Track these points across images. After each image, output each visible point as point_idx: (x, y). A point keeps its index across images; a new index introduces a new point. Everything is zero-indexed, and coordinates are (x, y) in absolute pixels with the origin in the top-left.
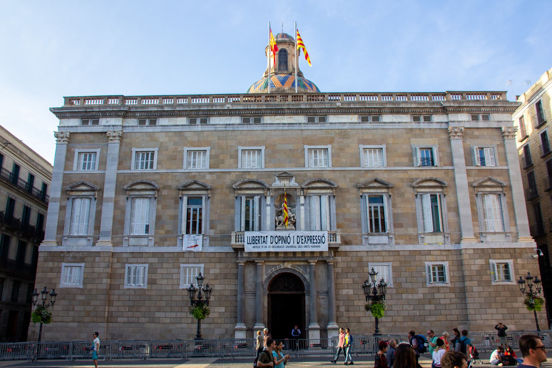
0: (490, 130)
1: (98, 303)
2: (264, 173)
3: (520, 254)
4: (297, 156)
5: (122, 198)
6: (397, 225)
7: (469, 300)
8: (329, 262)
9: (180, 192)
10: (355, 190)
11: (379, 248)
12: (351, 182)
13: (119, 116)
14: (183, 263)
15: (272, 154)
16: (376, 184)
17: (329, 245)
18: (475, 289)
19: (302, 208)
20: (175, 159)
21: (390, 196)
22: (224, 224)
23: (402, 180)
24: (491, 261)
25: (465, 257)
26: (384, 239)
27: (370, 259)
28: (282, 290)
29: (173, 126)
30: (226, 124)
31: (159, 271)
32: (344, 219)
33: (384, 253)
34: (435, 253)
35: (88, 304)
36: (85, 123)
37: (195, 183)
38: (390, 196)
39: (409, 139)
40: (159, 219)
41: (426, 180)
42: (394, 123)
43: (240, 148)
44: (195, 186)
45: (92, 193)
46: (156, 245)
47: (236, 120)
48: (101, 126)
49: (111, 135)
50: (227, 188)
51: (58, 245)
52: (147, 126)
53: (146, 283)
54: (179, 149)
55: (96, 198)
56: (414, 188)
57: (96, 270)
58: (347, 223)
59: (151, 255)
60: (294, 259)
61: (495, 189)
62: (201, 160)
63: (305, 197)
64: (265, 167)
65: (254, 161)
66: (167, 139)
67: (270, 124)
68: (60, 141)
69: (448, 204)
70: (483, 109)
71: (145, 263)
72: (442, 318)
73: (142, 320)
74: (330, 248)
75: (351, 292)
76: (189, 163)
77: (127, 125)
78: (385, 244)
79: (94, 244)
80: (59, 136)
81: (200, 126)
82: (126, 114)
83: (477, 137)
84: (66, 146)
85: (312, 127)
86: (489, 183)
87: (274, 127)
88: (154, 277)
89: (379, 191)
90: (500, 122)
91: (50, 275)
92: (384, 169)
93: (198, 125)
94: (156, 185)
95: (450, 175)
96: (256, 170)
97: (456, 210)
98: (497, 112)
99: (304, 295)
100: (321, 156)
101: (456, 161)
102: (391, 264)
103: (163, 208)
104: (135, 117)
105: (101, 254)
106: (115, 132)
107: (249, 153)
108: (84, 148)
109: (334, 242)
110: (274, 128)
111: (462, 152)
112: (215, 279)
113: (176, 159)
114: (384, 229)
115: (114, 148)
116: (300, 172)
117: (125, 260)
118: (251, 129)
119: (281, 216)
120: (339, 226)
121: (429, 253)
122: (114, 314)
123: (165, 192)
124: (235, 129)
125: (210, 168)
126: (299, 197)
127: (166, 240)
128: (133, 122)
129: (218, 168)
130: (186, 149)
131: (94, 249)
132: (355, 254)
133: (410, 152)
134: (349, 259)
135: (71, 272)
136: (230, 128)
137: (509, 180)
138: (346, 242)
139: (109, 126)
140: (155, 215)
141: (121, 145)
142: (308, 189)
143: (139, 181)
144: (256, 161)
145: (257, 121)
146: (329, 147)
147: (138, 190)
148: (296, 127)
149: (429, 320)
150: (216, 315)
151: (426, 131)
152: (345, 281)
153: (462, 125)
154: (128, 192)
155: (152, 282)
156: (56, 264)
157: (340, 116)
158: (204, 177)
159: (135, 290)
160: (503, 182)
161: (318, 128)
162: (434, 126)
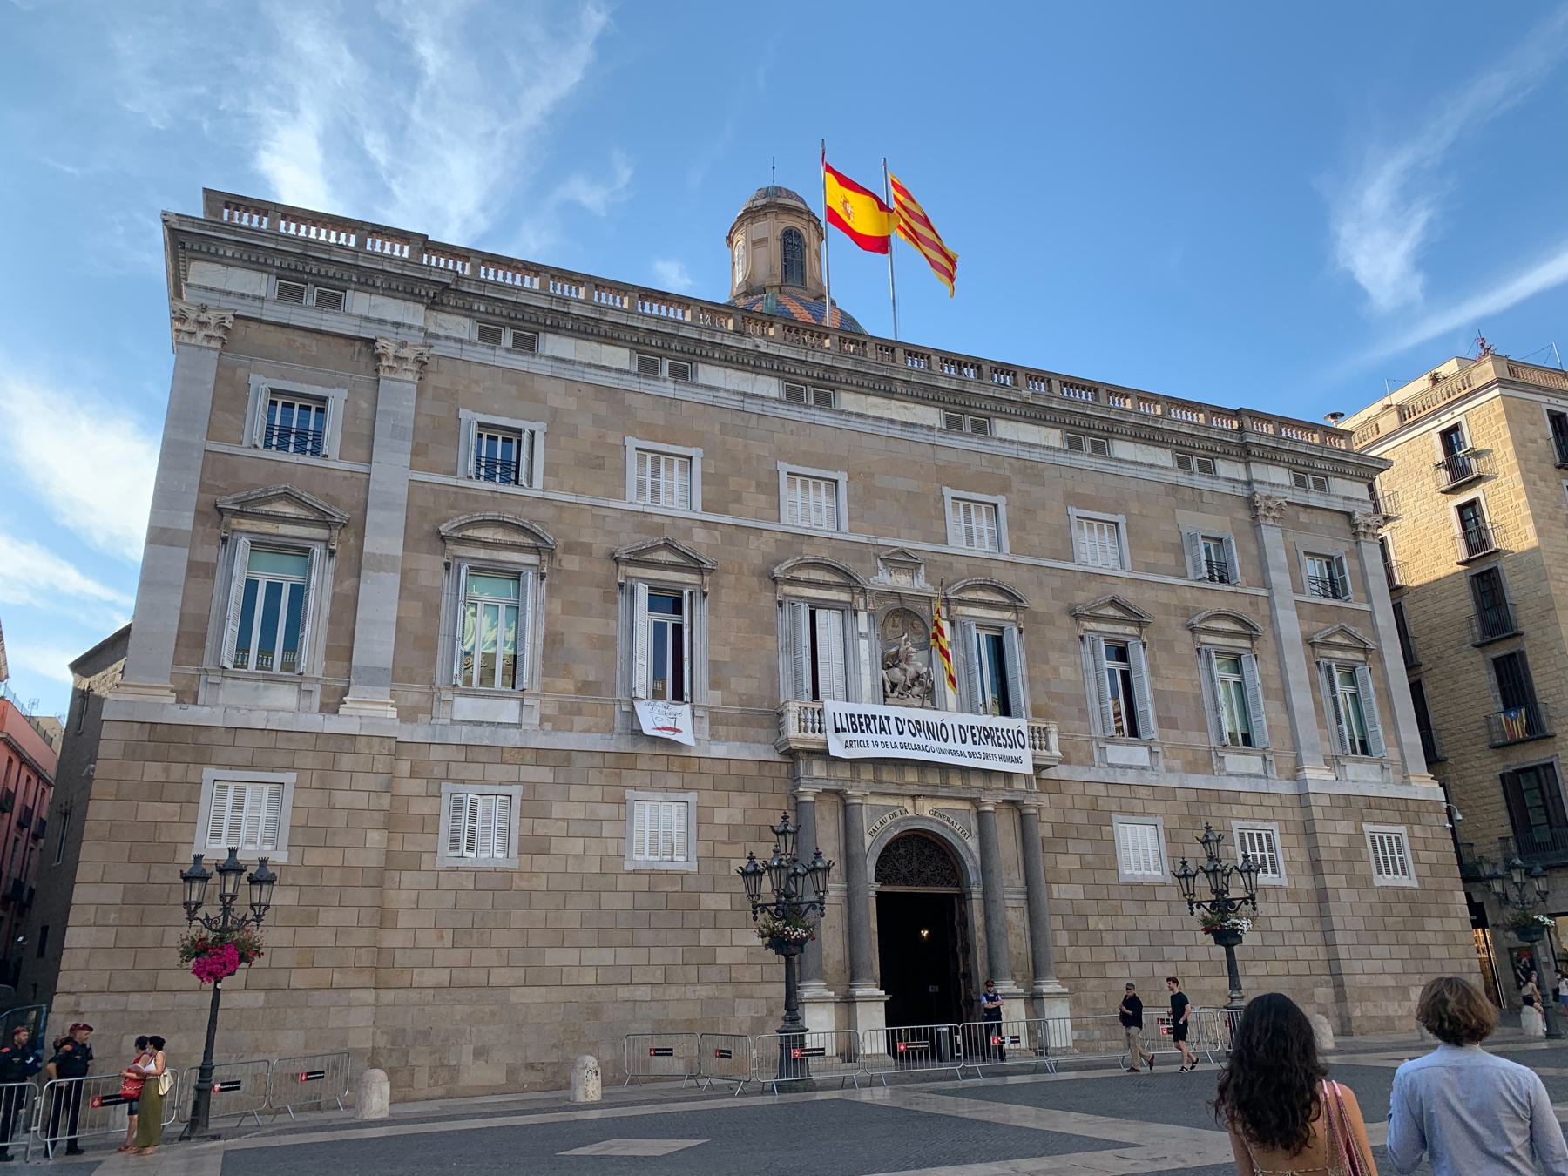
1: (349, 917)
2: (848, 546)
5: (429, 564)
6: (1165, 722)
7: (1337, 924)
8: (1029, 806)
9: (622, 568)
10: (1067, 621)
11: (1130, 778)
14: (635, 788)
15: (865, 499)
16: (1111, 612)
18: (1344, 894)
20: (601, 467)
23: (1165, 607)
24: (1368, 828)
25: (1317, 813)
26: (1139, 755)
28: (906, 882)
29: (590, 365)
30: (745, 394)
31: (558, 810)
33: (1143, 791)
34: (1249, 799)
35: (310, 921)
36: (290, 294)
37: (668, 546)
40: (554, 642)
41: (1219, 616)
42: (1141, 464)
43: (784, 467)
44: (663, 556)
45: (321, 533)
46: (548, 726)
47: (770, 387)
48: (351, 315)
49: (391, 351)
51: (179, 701)
52: (508, 350)
53: (514, 852)
54: (611, 441)
55: (332, 553)
56: (1192, 629)
57: (341, 799)
59: (529, 757)
60: (943, 792)
61: (1350, 656)
62: (676, 482)
63: (952, 624)
65: (818, 510)
66: (571, 403)
67: (857, 414)
68: (192, 334)
70: (1318, 464)
71: (510, 783)
72: (1279, 967)
73: (500, 976)
75: (1076, 892)
76: (641, 486)
77: (441, 332)
78: (1143, 768)
79: (331, 707)
80: (192, 316)
81: (670, 385)
82: (440, 296)
83: (1305, 528)
84: (216, 354)
85: (956, 441)
86: (1338, 639)
87: (867, 426)
88: (540, 831)
89: (1119, 629)
90: (1349, 499)
91: (150, 811)
92: (1126, 575)
93: (665, 380)
94: (550, 538)
95: (1263, 608)
98: (1342, 475)
99: (963, 897)
100: (981, 523)
102: (1160, 820)
103: (563, 613)
104: (467, 312)
105: (361, 745)
106: (403, 345)
107: (805, 486)
108: (283, 378)
110: (868, 429)
112: (731, 842)
114: (1134, 732)
115: (400, 397)
116: (936, 557)
117: (439, 771)
118: (809, 419)
121: (1235, 798)
122: (398, 953)
123: (571, 563)
124: (769, 410)
127: (580, 714)
128: (461, 326)
129: (726, 512)
130: (632, 443)
131: (332, 725)
132: (1078, 789)
133: (1176, 539)
135: (238, 804)
136: (754, 406)
137: (1377, 638)
139: (381, 321)
140: (541, 631)
141: (420, 392)
142: (962, 602)
143: (492, 514)
144: (824, 510)
145: (824, 401)
146: (1000, 500)
147: (485, 544)
148: (920, 436)
149: (1254, 971)
150: (740, 956)
151: (1207, 497)
152: (1065, 862)
153: (1276, 493)
154: (450, 547)
155: (534, 846)
156: (177, 771)
158: (688, 533)
159: (476, 873)
160: (1367, 640)
161: (973, 447)
162: (1226, 488)
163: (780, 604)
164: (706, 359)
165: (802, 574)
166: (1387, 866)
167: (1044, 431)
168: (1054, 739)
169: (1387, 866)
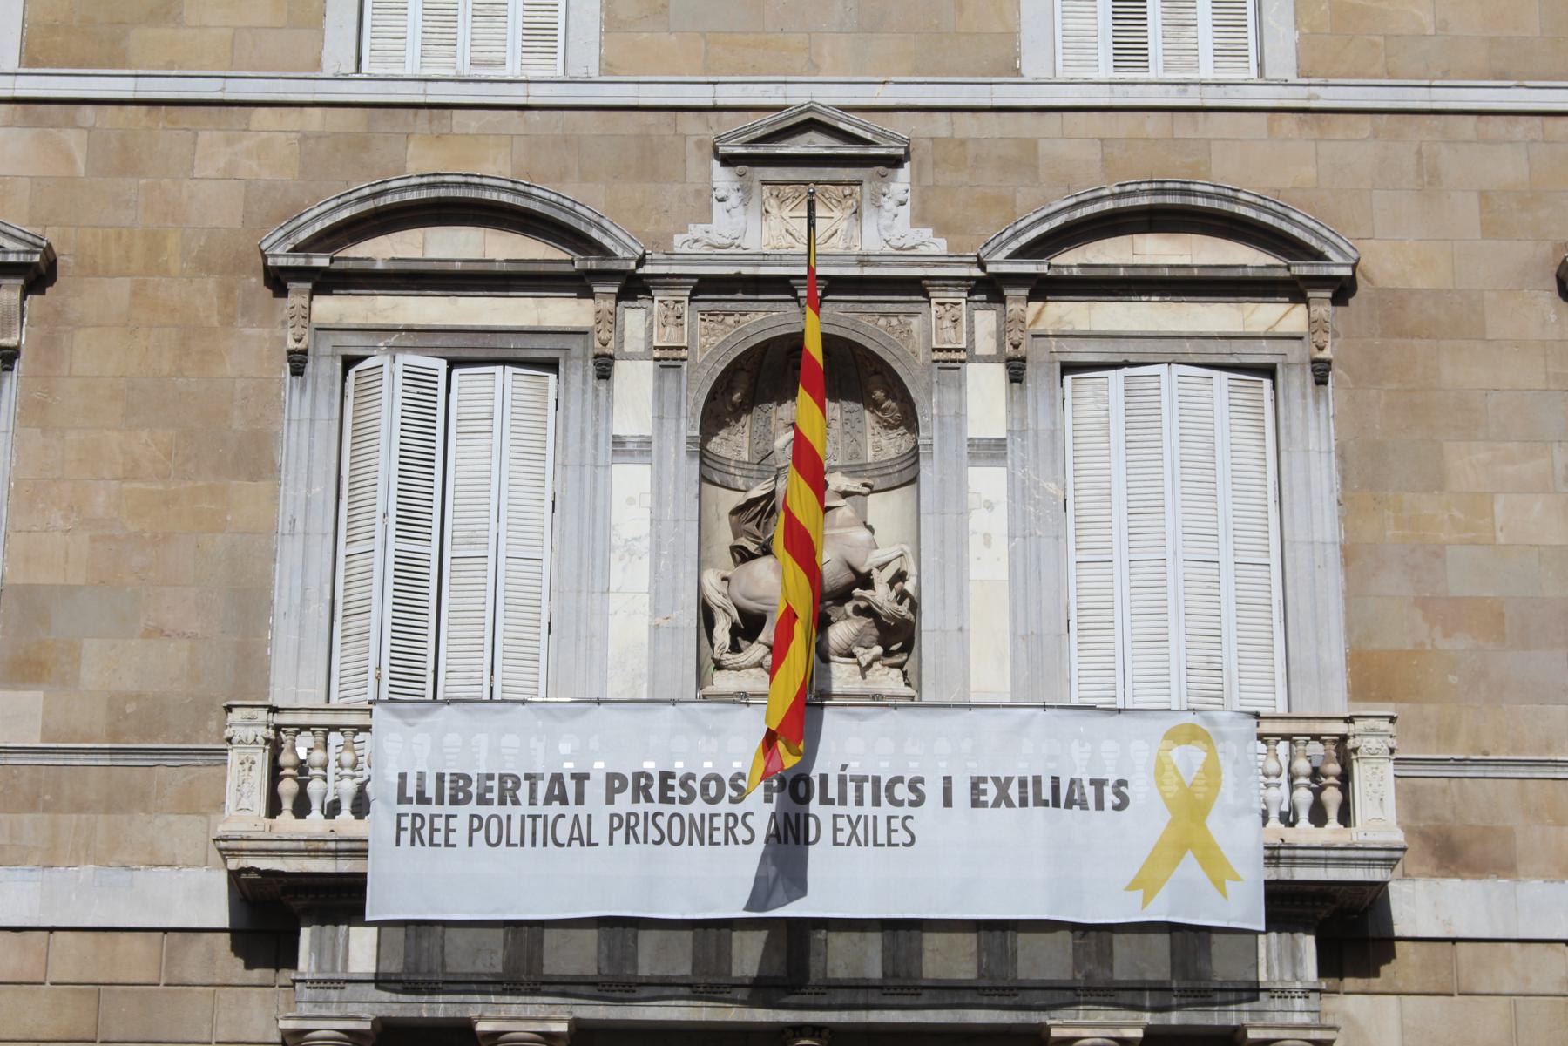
12: (1492, 228)
17: (1273, 856)
19: (988, 481)
22: (158, 632)
32: (1423, 603)
50: (204, 265)
58: (1460, 643)
63: (1016, 371)
64: (607, 66)
74: (1289, 905)
96: (516, 95)
109: (1332, 832)
119: (762, 566)
120: (1371, 676)
125: (32, 58)
129: (115, 59)
138: (1450, 852)
163: (298, 362)
165: (381, 250)
168: (1375, 785)
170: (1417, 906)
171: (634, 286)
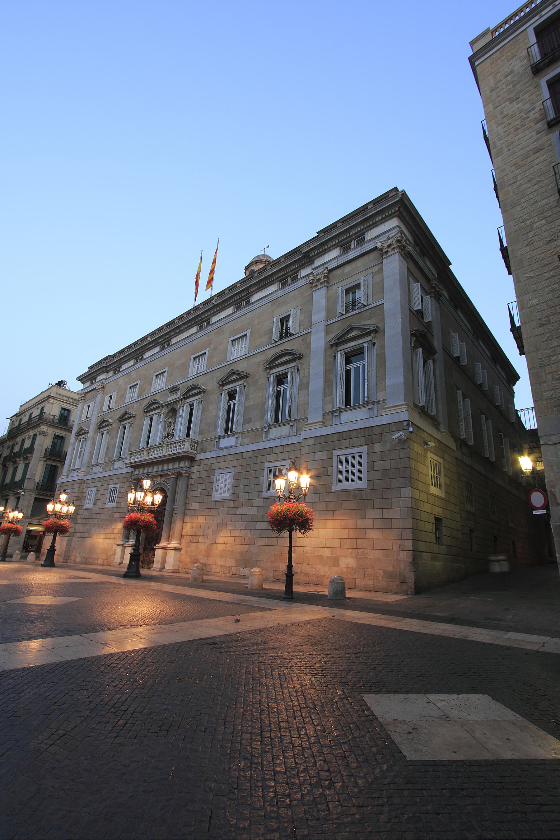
0: (366, 258)
3: (380, 434)
4: (185, 366)
13: (103, 372)
16: (234, 377)
21: (245, 386)
24: (335, 453)
27: (217, 466)
33: (230, 458)
34: (276, 450)
38: (245, 386)
39: (273, 312)
69: (300, 380)
78: (231, 447)
82: (106, 369)
86: (353, 334)
92: (244, 357)
97: (305, 386)
98: (376, 225)
101: (315, 318)
104: (111, 370)
111: (323, 302)
113: (123, 396)
120: (201, 433)
126: (179, 408)
128: (111, 374)
134: (201, 468)
138: (203, 451)
140: (106, 446)
157: (220, 314)
164: (145, 352)
166: (347, 476)
167: (227, 310)
169: (347, 476)
170: (198, 457)
171: (163, 407)
